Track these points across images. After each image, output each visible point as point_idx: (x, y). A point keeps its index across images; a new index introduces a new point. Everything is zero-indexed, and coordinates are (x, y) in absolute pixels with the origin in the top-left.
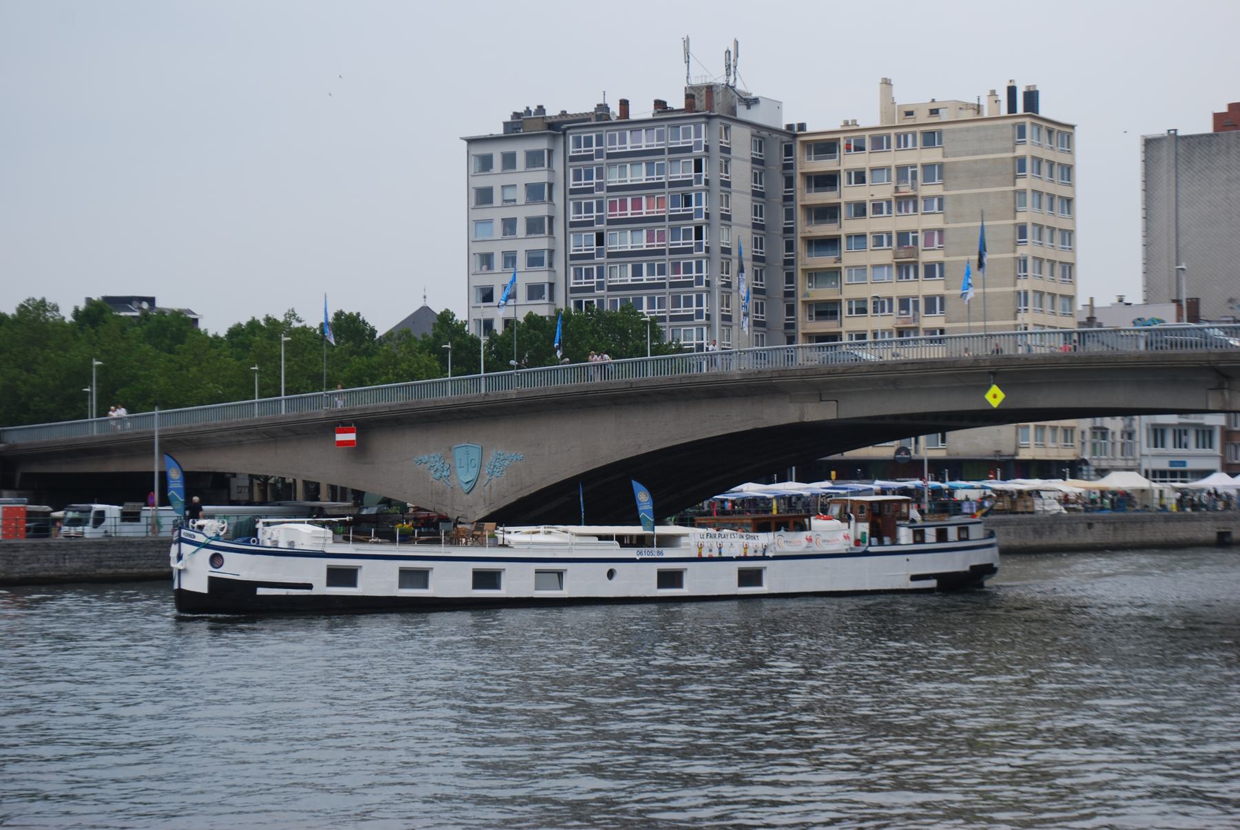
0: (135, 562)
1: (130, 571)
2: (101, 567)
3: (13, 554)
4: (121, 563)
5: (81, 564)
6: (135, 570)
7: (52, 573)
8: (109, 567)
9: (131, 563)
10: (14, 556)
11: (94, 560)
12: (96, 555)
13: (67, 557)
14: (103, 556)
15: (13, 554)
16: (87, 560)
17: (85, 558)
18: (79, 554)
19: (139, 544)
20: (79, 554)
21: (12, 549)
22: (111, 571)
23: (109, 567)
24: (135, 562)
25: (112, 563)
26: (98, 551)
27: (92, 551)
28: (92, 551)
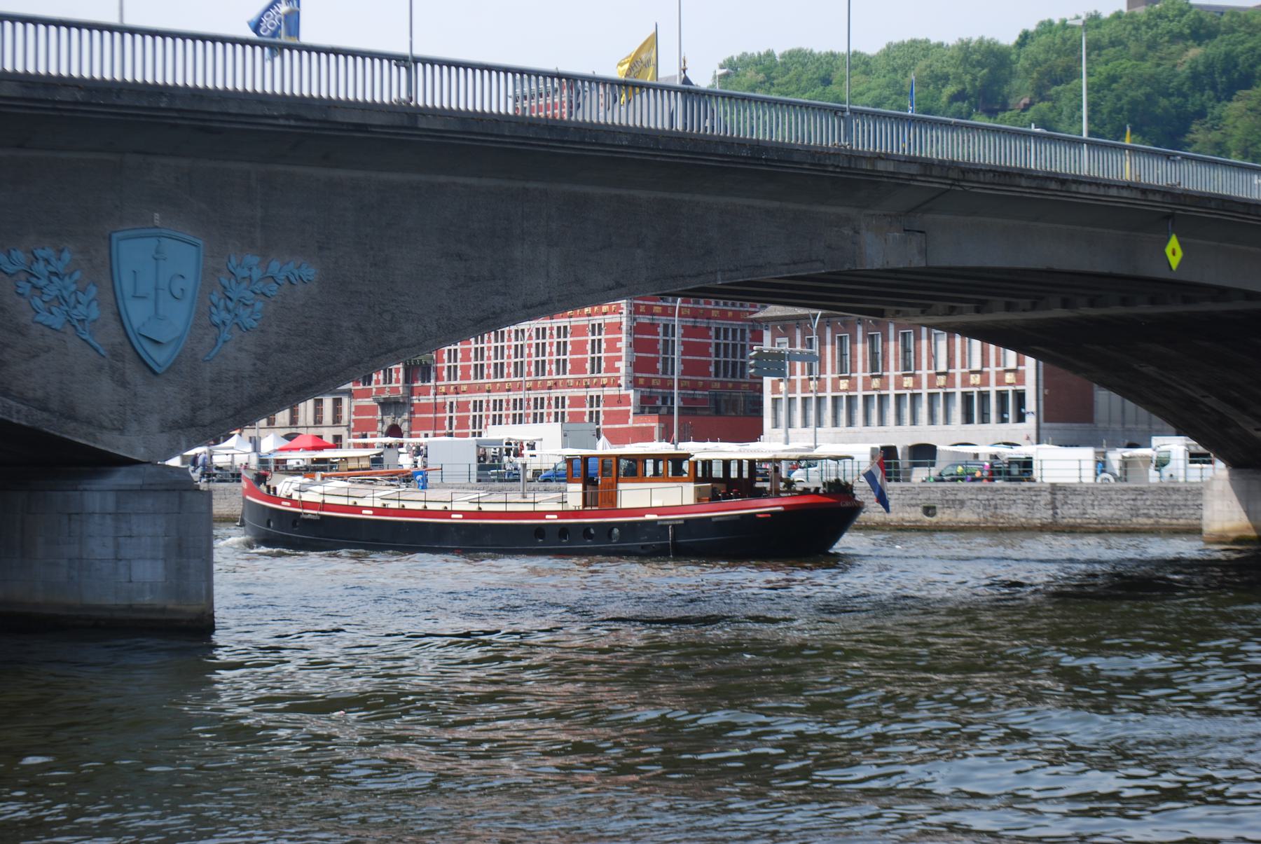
0: (1181, 512)
1: (1174, 522)
2: (1138, 516)
3: (1034, 498)
4: (1164, 512)
5: (1112, 512)
6: (1182, 521)
7: (1079, 521)
8: (1148, 516)
9: (1177, 512)
10: (1035, 501)
11: (1128, 507)
12: (1132, 502)
13: (1096, 503)
14: (1139, 503)
15: (1034, 498)
16: (1121, 508)
17: (1117, 505)
18: (1111, 500)
19: (1187, 491)
20: (1111, 500)
21: (1032, 493)
22: (1151, 521)
23: (1148, 516)
24: (1181, 512)
25: (1152, 512)
26: (1133, 497)
27: (1126, 497)
28: (1126, 497)
